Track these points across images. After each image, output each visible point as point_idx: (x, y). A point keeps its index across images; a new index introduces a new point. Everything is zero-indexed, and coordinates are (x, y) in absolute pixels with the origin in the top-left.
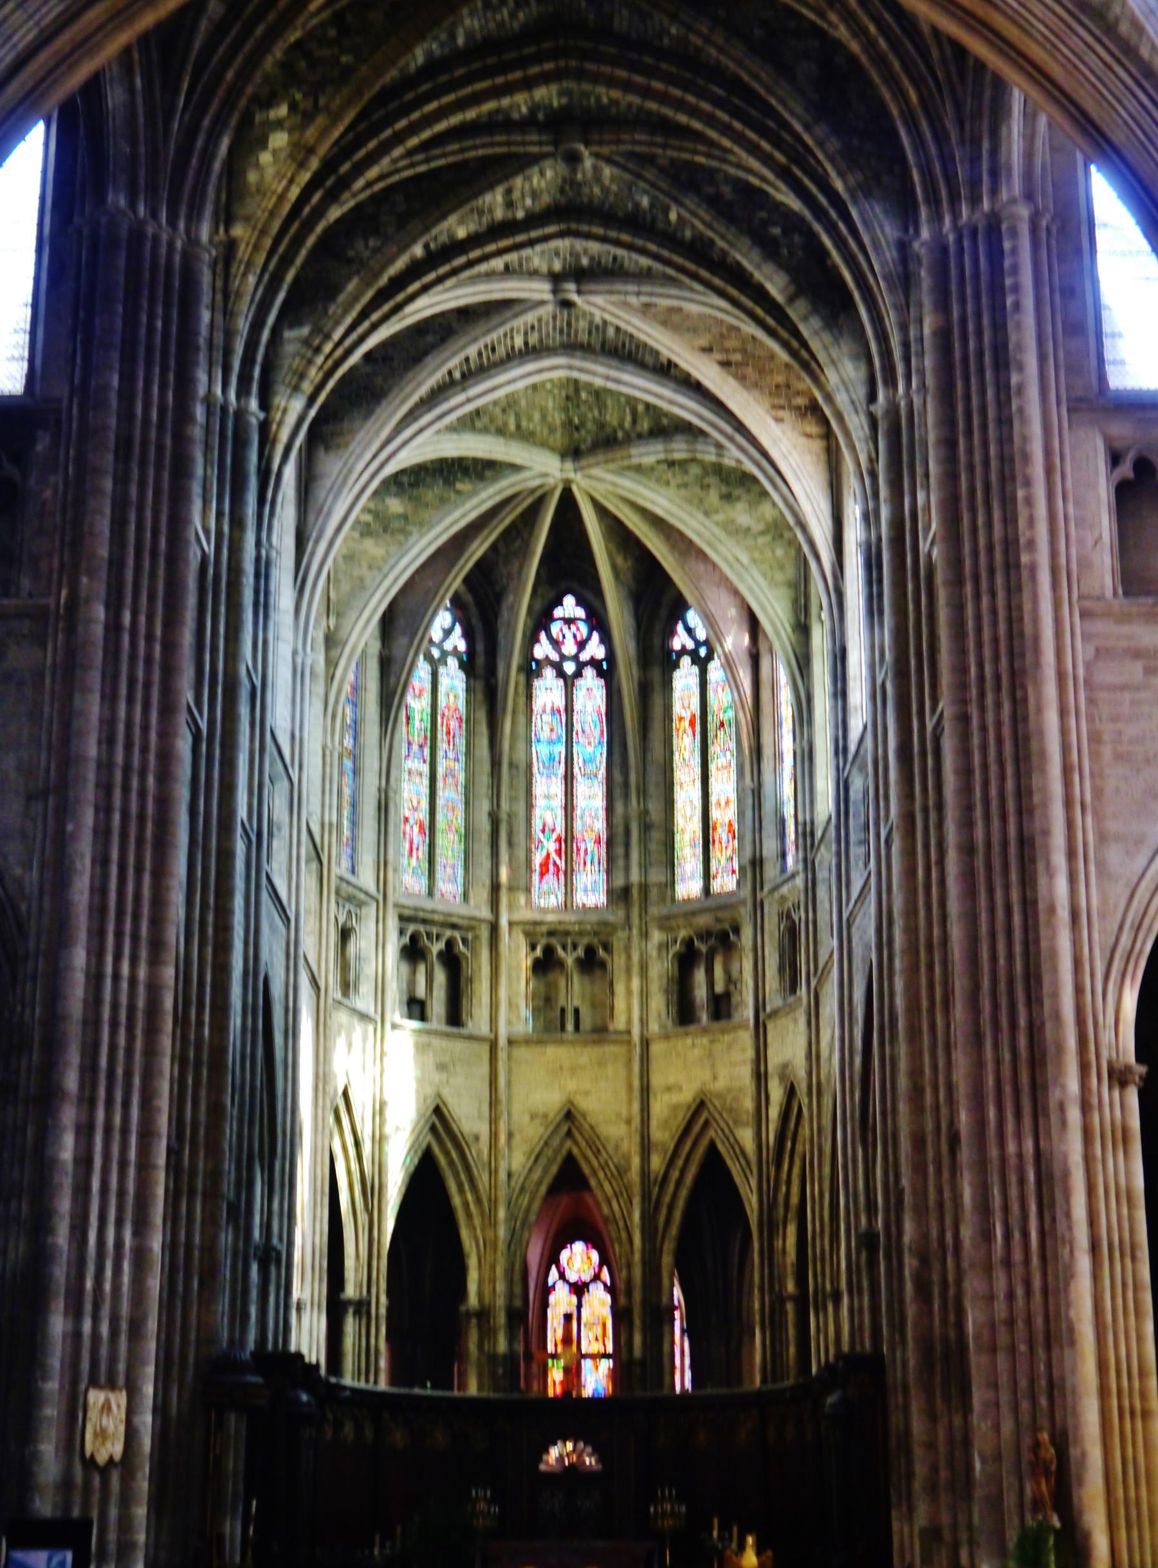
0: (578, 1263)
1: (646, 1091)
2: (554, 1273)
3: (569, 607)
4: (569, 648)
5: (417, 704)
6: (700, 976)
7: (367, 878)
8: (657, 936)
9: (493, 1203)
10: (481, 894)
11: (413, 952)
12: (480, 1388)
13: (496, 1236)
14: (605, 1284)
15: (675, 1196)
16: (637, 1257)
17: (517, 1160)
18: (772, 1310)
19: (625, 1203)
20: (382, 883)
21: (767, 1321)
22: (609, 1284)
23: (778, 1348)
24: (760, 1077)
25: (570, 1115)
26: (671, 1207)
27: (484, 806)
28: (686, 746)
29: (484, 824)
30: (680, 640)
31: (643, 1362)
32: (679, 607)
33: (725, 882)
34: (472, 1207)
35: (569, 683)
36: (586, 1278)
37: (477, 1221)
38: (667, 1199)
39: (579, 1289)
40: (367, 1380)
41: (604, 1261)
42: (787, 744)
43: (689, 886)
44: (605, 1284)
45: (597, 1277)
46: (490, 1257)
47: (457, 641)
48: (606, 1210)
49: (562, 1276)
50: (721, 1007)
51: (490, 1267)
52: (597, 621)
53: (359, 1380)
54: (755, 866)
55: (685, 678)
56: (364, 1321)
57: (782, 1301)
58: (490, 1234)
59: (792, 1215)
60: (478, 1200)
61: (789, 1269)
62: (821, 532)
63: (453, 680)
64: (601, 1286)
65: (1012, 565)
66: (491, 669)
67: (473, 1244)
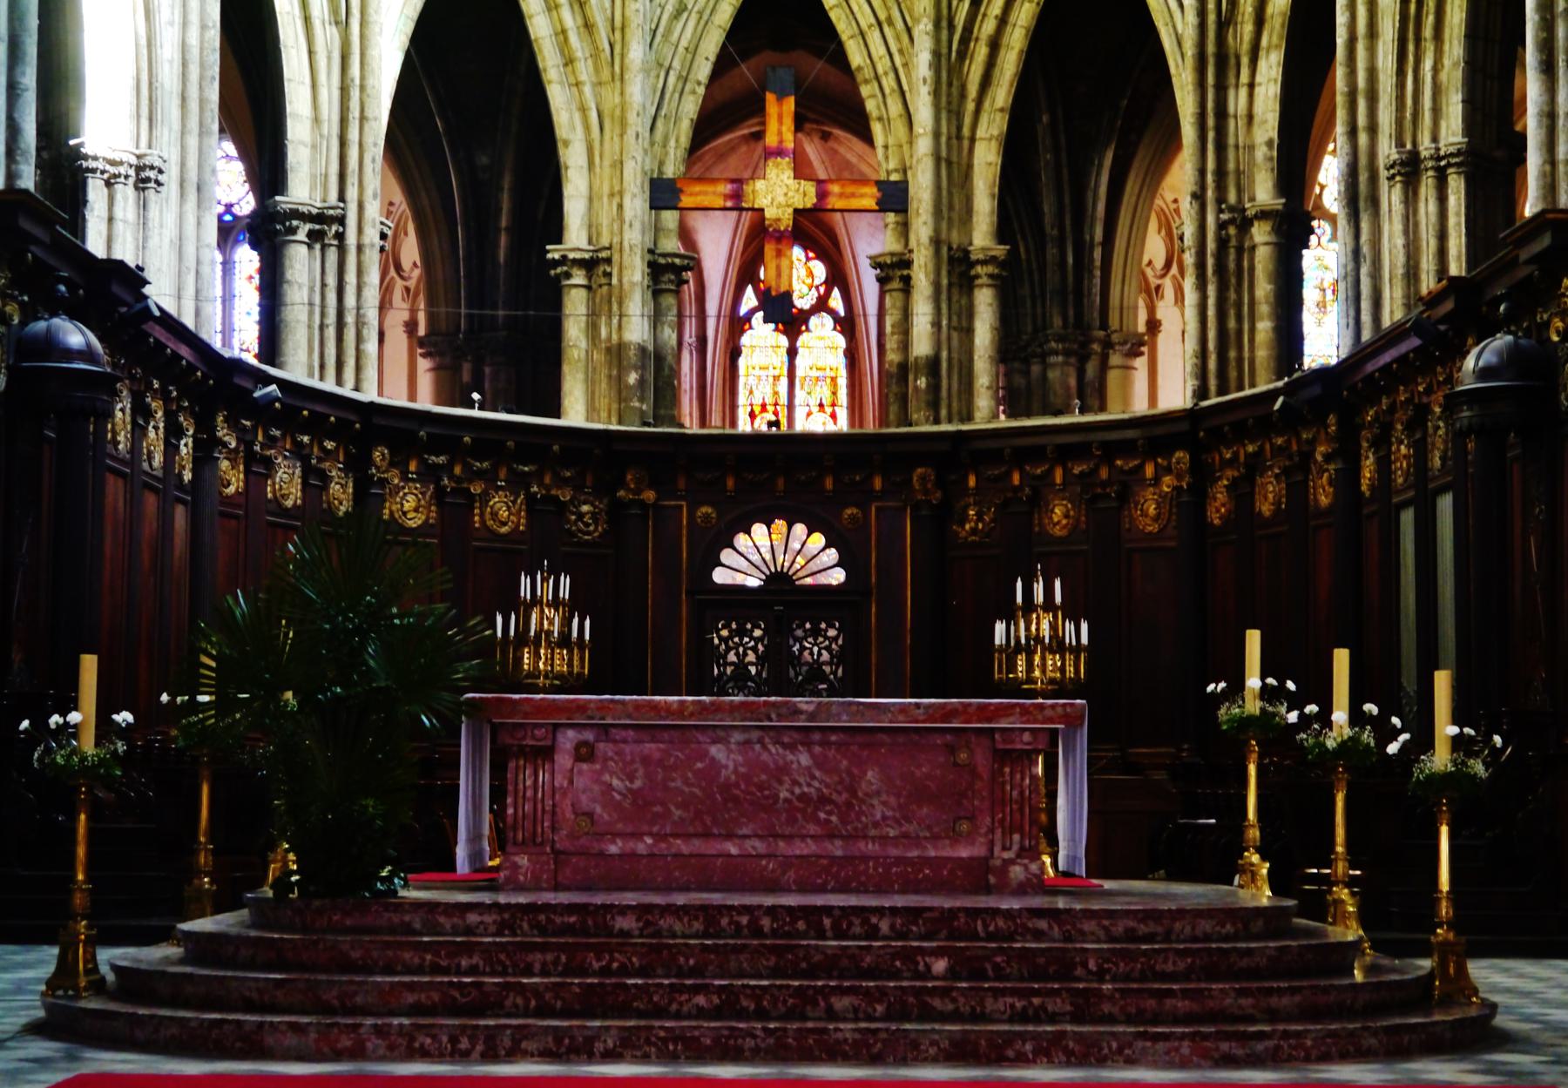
9: (619, 28)
12: (592, 410)
13: (623, 107)
14: (832, 313)
15: (1003, 21)
16: (924, 145)
18: (1222, 243)
19: (898, 38)
21: (1210, 262)
22: (842, 313)
23: (1232, 324)
26: (995, 45)
31: (933, 365)
34: (574, 39)
37: (584, 71)
38: (988, 27)
40: (339, 382)
41: (838, 277)
45: (821, 305)
46: (611, 147)
48: (856, 57)
51: (613, 166)
53: (322, 378)
56: (332, 255)
57: (1245, 224)
58: (611, 98)
59: (1274, 34)
60: (588, 26)
61: (1261, 152)
64: (828, 320)
67: (577, 116)
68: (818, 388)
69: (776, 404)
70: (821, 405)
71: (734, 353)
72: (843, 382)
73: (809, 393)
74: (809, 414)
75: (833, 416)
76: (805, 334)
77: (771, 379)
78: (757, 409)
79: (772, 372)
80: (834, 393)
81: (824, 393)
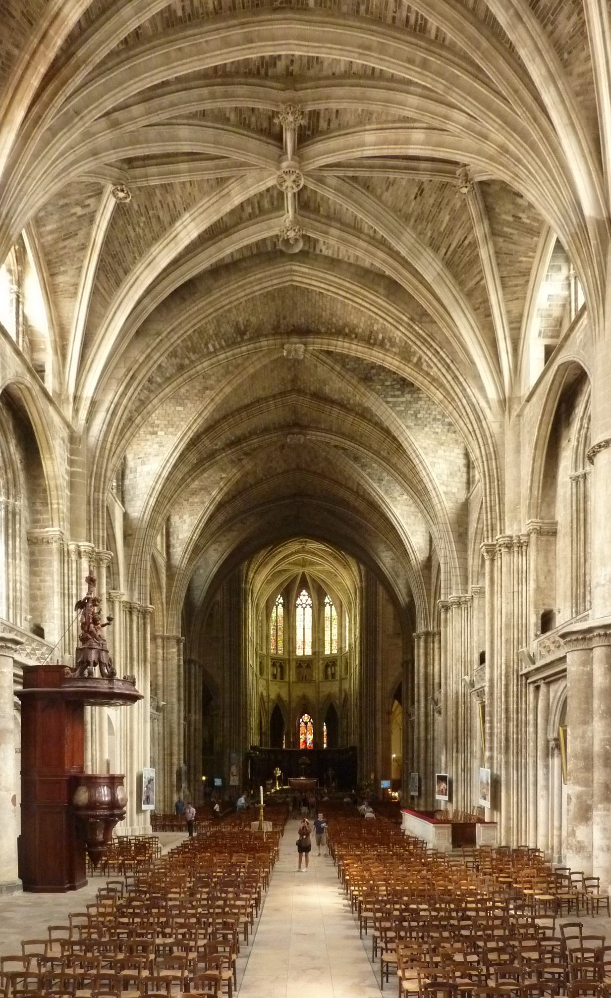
1: (319, 692)
3: (304, 592)
4: (304, 601)
5: (274, 615)
6: (329, 669)
7: (264, 652)
8: (321, 662)
10: (286, 653)
11: (274, 665)
17: (293, 705)
20: (268, 653)
24: (340, 690)
25: (304, 697)
27: (287, 636)
28: (327, 623)
29: (287, 638)
30: (327, 600)
32: (326, 595)
33: (335, 651)
35: (304, 609)
39: (306, 723)
42: (347, 624)
43: (327, 652)
47: (281, 601)
50: (333, 675)
52: (310, 595)
54: (340, 649)
55: (327, 608)
62: (352, 591)
63: (281, 609)
65: (376, 631)
66: (288, 607)
71: (299, 727)
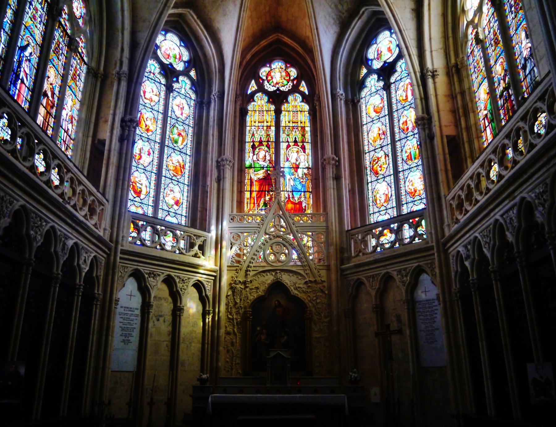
0: (277, 76)
2: (253, 86)
14: (302, 94)
36: (285, 89)
44: (302, 94)
45: (295, 89)
49: (261, 89)
64: (299, 97)
68: (293, 133)
69: (268, 141)
70: (296, 142)
71: (244, 113)
72: (308, 129)
73: (288, 135)
74: (288, 146)
75: (303, 148)
76: (286, 105)
77: (265, 128)
78: (257, 144)
79: (265, 124)
80: (303, 135)
81: (298, 135)
